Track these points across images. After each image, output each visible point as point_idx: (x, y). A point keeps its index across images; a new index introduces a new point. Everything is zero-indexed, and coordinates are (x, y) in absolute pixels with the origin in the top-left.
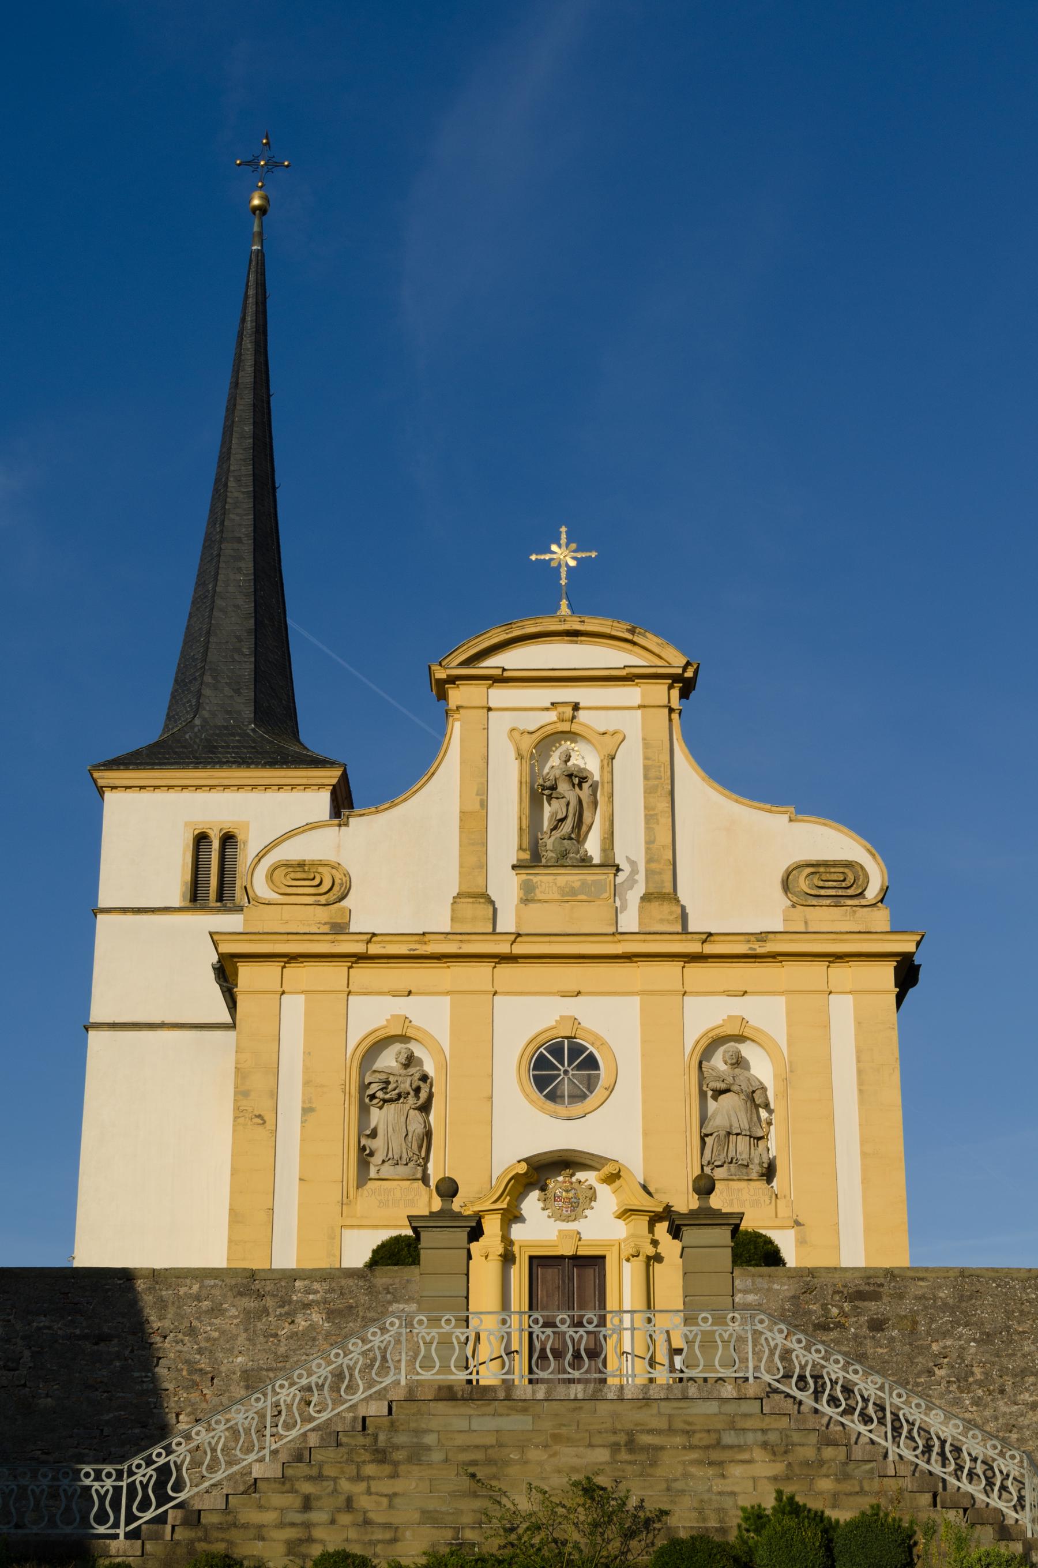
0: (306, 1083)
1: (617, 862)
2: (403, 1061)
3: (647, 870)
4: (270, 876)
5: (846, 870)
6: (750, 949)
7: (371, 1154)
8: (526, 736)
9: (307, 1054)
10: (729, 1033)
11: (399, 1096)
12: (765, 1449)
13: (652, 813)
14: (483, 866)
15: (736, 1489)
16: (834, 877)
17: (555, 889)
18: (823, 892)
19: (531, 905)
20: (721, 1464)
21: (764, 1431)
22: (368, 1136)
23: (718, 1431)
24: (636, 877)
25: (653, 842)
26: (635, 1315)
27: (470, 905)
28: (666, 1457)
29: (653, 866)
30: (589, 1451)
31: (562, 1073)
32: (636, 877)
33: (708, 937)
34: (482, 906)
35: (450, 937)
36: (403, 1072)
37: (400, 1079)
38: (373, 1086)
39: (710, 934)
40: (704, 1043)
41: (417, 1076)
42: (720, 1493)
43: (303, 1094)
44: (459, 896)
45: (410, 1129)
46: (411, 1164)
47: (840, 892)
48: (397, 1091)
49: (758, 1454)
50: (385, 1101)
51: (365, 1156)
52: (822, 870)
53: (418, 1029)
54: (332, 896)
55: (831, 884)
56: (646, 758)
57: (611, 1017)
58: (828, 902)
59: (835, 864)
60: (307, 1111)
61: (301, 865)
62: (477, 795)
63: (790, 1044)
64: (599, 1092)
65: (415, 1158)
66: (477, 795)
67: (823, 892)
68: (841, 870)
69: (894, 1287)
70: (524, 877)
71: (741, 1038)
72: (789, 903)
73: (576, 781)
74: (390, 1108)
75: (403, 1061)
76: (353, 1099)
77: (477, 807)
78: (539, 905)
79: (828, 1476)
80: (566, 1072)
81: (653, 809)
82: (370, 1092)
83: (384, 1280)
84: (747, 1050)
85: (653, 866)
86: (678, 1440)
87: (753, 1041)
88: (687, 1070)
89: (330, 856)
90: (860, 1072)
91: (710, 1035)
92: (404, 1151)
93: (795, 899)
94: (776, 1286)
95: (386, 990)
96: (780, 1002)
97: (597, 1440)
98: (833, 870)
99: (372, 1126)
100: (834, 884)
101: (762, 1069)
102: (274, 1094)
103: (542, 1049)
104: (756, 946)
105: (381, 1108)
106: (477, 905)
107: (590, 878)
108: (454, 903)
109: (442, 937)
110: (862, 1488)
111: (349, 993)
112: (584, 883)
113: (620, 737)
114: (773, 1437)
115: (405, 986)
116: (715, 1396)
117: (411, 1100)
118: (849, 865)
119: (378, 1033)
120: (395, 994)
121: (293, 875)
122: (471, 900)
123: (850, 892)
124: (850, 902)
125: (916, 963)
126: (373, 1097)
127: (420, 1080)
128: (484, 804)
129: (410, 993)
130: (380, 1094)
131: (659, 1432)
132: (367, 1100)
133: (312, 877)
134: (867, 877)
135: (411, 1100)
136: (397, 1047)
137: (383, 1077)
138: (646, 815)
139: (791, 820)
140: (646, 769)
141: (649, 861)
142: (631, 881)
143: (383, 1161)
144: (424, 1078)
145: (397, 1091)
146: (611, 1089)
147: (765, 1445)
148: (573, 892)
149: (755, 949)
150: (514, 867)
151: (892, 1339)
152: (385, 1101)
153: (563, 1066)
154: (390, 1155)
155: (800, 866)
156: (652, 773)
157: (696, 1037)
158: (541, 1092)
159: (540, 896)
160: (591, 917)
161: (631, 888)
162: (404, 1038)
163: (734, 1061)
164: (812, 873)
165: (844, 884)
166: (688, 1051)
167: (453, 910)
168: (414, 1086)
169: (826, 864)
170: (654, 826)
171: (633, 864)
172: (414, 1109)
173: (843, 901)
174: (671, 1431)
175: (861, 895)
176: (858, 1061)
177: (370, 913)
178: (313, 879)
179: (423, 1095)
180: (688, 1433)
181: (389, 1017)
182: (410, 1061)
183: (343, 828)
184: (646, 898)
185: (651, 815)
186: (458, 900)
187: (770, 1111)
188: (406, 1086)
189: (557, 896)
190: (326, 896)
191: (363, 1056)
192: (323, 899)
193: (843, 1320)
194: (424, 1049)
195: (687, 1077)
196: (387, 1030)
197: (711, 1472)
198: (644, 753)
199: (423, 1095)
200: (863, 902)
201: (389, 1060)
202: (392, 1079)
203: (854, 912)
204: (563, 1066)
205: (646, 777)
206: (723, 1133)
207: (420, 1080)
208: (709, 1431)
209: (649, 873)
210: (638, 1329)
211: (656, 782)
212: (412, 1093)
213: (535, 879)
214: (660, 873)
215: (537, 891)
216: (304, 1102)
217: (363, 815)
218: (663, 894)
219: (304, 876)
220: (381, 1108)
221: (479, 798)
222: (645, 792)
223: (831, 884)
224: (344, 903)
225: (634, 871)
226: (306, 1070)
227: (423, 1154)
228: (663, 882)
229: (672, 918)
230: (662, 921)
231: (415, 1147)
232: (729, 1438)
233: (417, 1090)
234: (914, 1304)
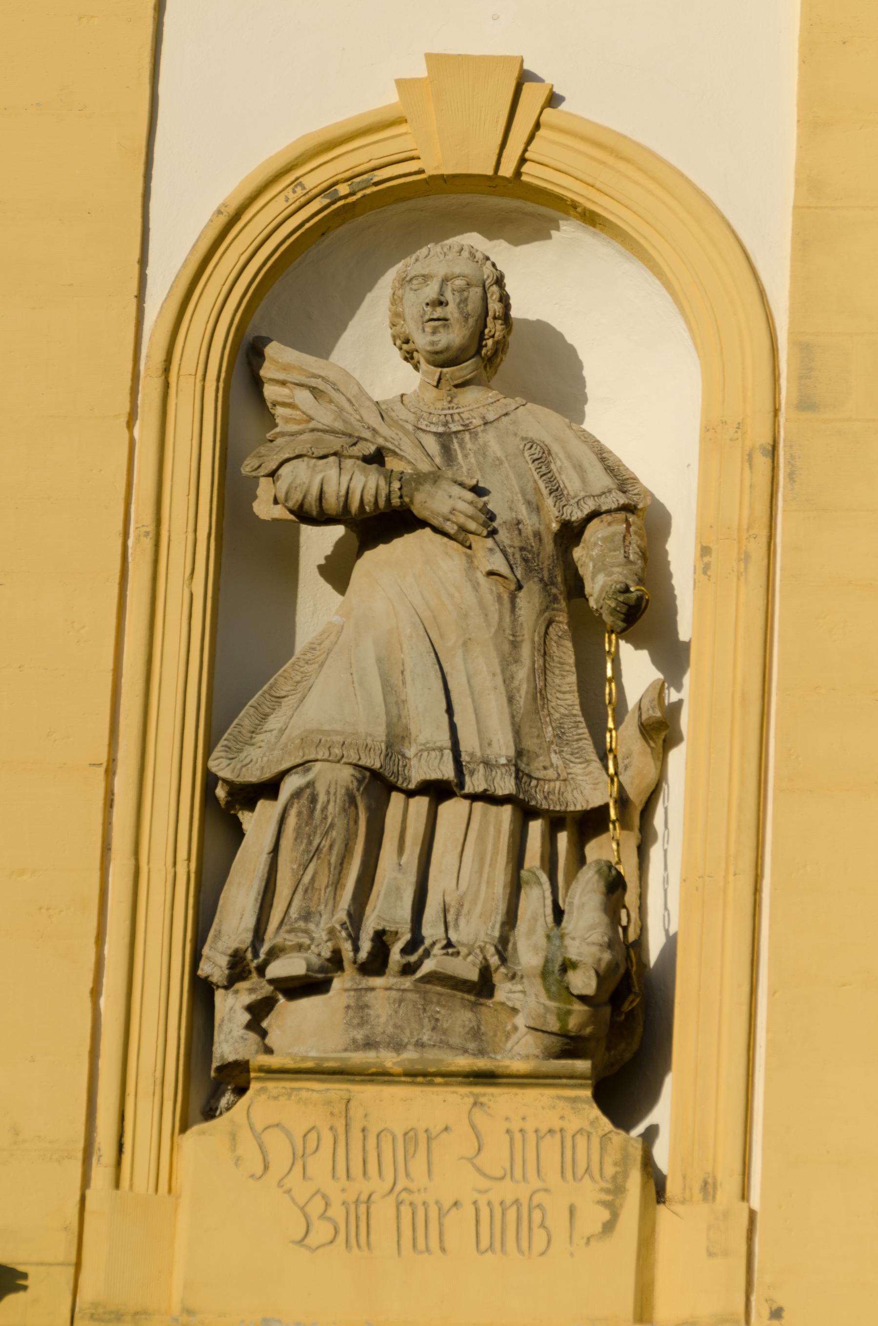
10: (436, 163)
40: (273, 222)
71: (517, 205)
84: (547, 283)
87: (591, 219)
88: (150, 388)
101: (647, 405)
163: (454, 336)
187: (672, 658)
195: (145, 431)
206: (333, 779)
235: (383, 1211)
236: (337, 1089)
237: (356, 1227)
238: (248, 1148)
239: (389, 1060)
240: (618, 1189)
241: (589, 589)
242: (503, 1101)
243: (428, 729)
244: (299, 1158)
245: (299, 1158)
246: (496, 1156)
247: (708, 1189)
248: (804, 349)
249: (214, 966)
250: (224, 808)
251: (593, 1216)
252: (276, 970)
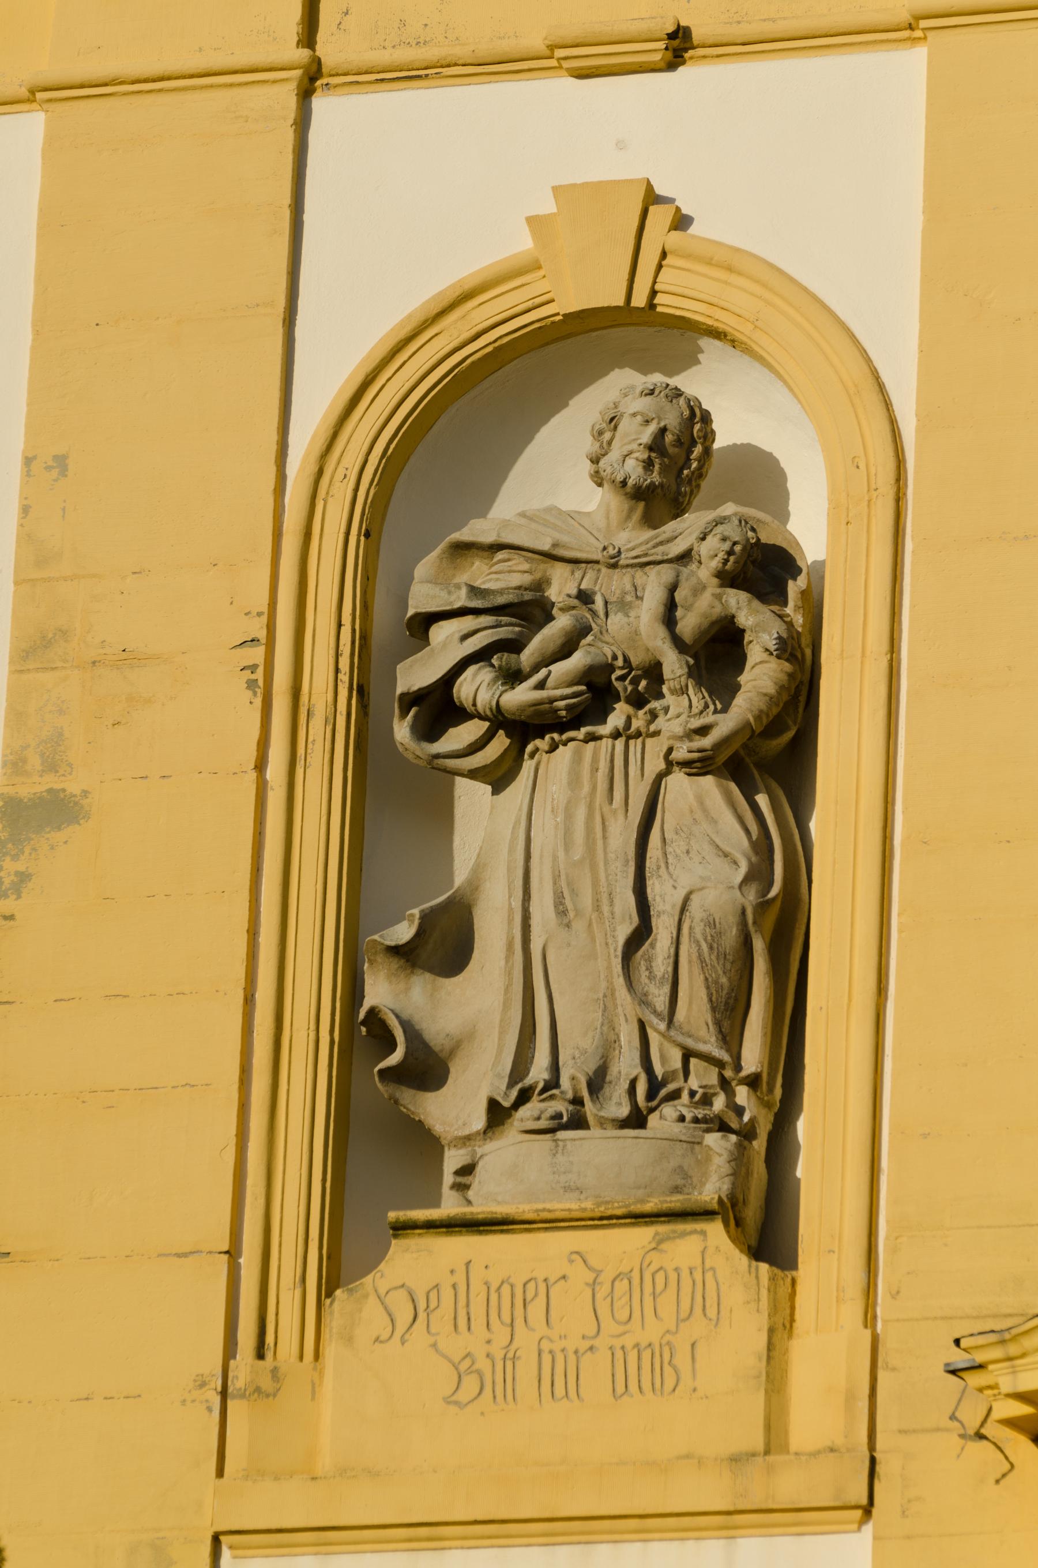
2: (633, 470)
7: (427, 1069)
11: (597, 694)
22: (406, 955)
36: (632, 539)
37: (608, 585)
38: (441, 632)
41: (712, 554)
43: (16, 716)
45: (663, 895)
46: (664, 1121)
48: (577, 661)
50: (525, 729)
51: (382, 1073)
53: (728, 262)
65: (702, 1077)
74: (556, 769)
75: (633, 470)
76: (317, 729)
82: (418, 673)
92: (628, 1037)
95: (536, 43)
99: (460, 878)
105: (499, 777)
111: (311, 80)
117: (680, 710)
120: (591, 61)
126: (438, 708)
127: (729, 579)
129: (679, 46)
130: (477, 687)
132: (402, 731)
135: (680, 711)
136: (619, 396)
137: (504, 578)
143: (497, 1115)
144: (765, 568)
145: (577, 661)
152: (525, 729)
154: (538, 1072)
162: (642, 331)
168: (688, 624)
172: (700, 766)
179: (760, 676)
181: (547, 206)
182: (676, 467)
188: (633, 627)
191: (394, 467)
194: (780, 395)
196: (536, 286)
199: (760, 676)
201: (559, 482)
202: (561, 586)
207: (729, 579)
212: (673, 665)
220: (499, 777)
227: (753, 1055)
231: (695, 1009)
233: (718, 654)
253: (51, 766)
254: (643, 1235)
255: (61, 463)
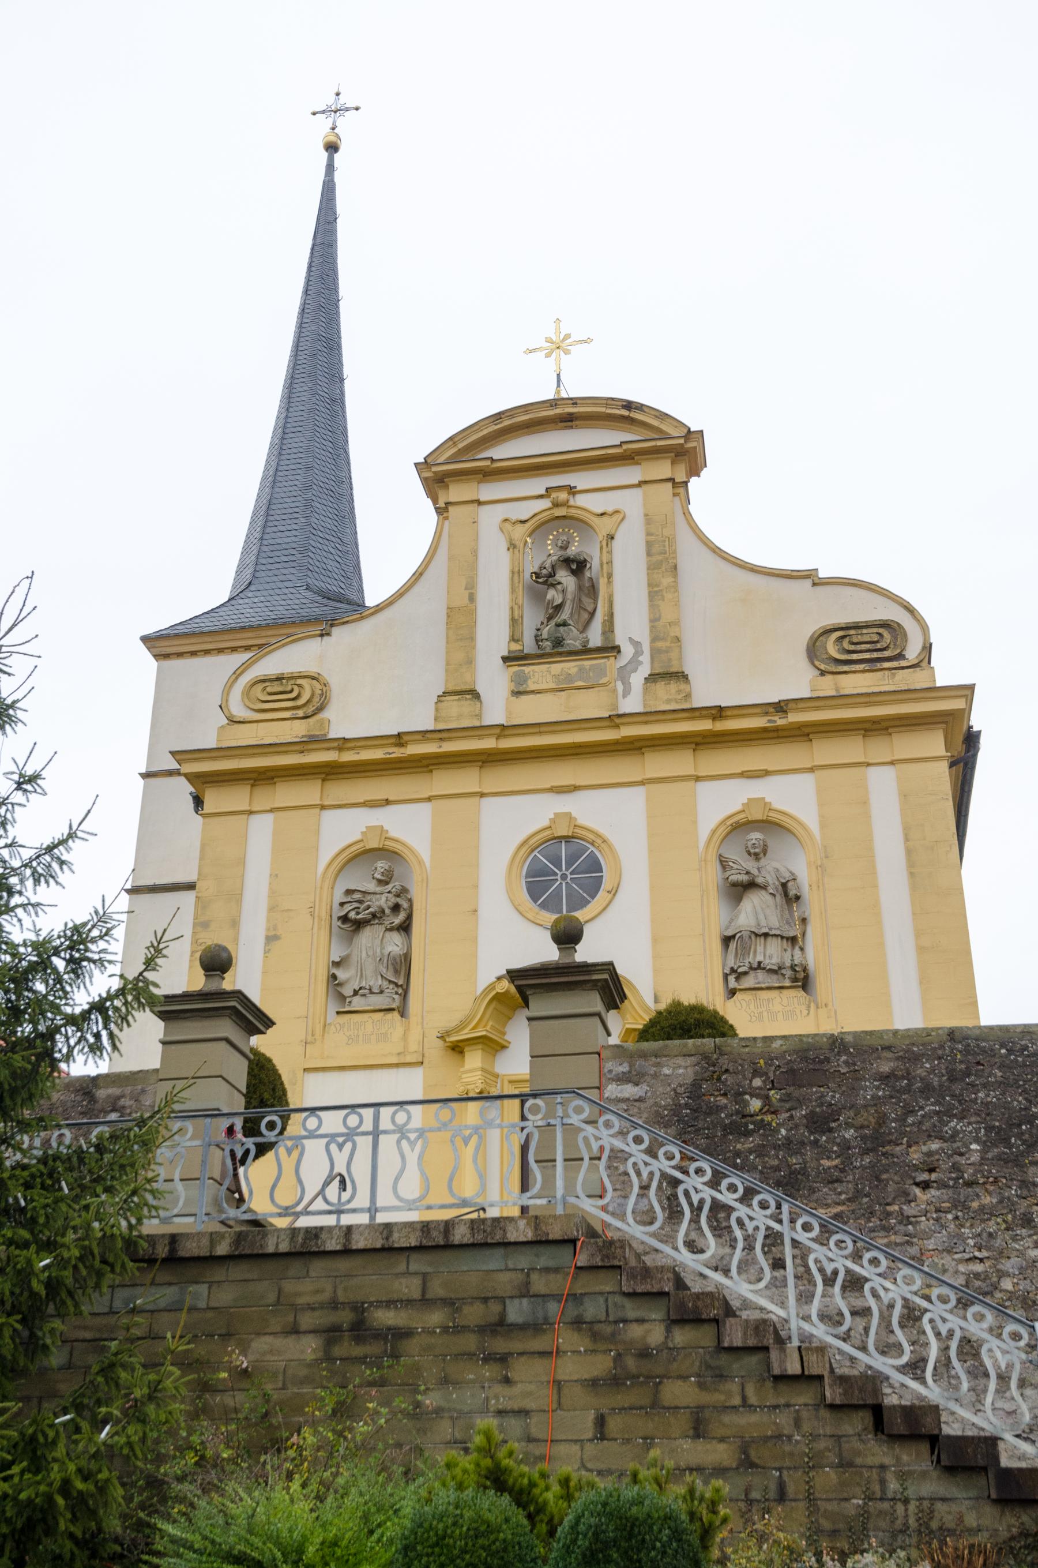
0: (272, 909)
1: (617, 643)
3: (652, 649)
4: (247, 692)
5: (881, 630)
6: (769, 721)
8: (520, 526)
9: (274, 876)
12: (579, 1330)
13: (656, 589)
14: (470, 661)
15: (530, 1404)
16: (867, 638)
17: (549, 678)
18: (855, 657)
19: (524, 698)
20: (503, 1359)
21: (576, 1298)
23: (502, 1300)
24: (641, 658)
25: (659, 619)
26: (382, 1110)
27: (455, 703)
28: (413, 1345)
29: (659, 644)
30: (290, 1341)
31: (559, 877)
32: (641, 658)
33: (719, 712)
34: (469, 702)
35: (428, 735)
39: (720, 709)
42: (500, 1413)
43: (268, 921)
44: (446, 694)
47: (875, 655)
49: (566, 1339)
52: (852, 632)
54: (310, 709)
55: (863, 647)
56: (648, 534)
57: (614, 812)
58: (861, 667)
59: (868, 625)
60: (271, 939)
61: (279, 679)
62: (466, 589)
63: (823, 826)
64: (602, 896)
66: (466, 589)
67: (855, 657)
68: (875, 630)
69: (846, 1063)
70: (516, 668)
72: (818, 673)
73: (574, 567)
77: (466, 601)
78: (531, 696)
79: (684, 1378)
80: (564, 877)
81: (658, 586)
83: (110, 1091)
85: (659, 644)
86: (436, 1318)
89: (312, 669)
90: (909, 852)
91: (729, 823)
93: (823, 667)
94: (666, 1071)
96: (807, 781)
97: (307, 1320)
98: (865, 631)
100: (868, 646)
102: (235, 923)
103: (536, 853)
104: (776, 718)
106: (463, 702)
107: (587, 664)
108: (439, 701)
109: (419, 737)
110: (744, 1398)
112: (581, 669)
113: (621, 516)
114: (592, 1310)
115: (381, 796)
116: (498, 1237)
118: (885, 625)
119: (353, 849)
121: (269, 689)
122: (457, 697)
123: (886, 654)
124: (887, 665)
125: (975, 729)
128: (472, 598)
131: (409, 1302)
133: (289, 688)
134: (905, 635)
138: (650, 592)
139: (814, 584)
140: (649, 545)
141: (654, 639)
142: (634, 663)
146: (614, 892)
147: (577, 1323)
148: (569, 678)
149: (775, 722)
150: (505, 659)
151: (846, 1146)
153: (561, 870)
155: (828, 632)
156: (656, 548)
157: (713, 825)
158: (535, 902)
159: (532, 687)
160: (590, 705)
161: (635, 670)
164: (843, 637)
165: (879, 646)
166: (702, 844)
167: (437, 710)
169: (857, 626)
170: (660, 602)
171: (636, 644)
173: (879, 665)
174: (425, 1302)
175: (900, 656)
176: (907, 839)
177: (345, 720)
178: (292, 691)
180: (450, 1303)
183: (325, 638)
184: (653, 678)
185: (656, 592)
186: (443, 698)
189: (552, 686)
190: (305, 709)
192: (300, 713)
193: (768, 1118)
197: (488, 1372)
198: (647, 529)
200: (903, 663)
203: (894, 675)
204: (561, 870)
205: (649, 554)
208: (485, 1300)
209: (655, 653)
210: (385, 1132)
211: (660, 558)
213: (527, 669)
214: (667, 652)
215: (530, 682)
216: (268, 929)
217: (347, 622)
218: (669, 675)
219: (280, 689)
221: (468, 592)
222: (648, 569)
223: (863, 647)
224: (325, 715)
225: (638, 653)
226: (273, 893)
228: (670, 660)
229: (680, 697)
230: (669, 701)
232: (517, 1312)
234: (878, 1088)
235: (765, 1014)
236: (754, 992)
237: (760, 1017)
238: (738, 1004)
239: (763, 986)
240: (809, 1007)
241: (789, 896)
242: (785, 992)
243: (763, 922)
244: (748, 1005)
245: (748, 1005)
246: (785, 1002)
247: (826, 1005)
248: (825, 847)
249: (727, 971)
250: (727, 940)
251: (805, 1012)
252: (739, 970)
253: (275, 930)
254: (381, 1014)
255: (277, 875)
